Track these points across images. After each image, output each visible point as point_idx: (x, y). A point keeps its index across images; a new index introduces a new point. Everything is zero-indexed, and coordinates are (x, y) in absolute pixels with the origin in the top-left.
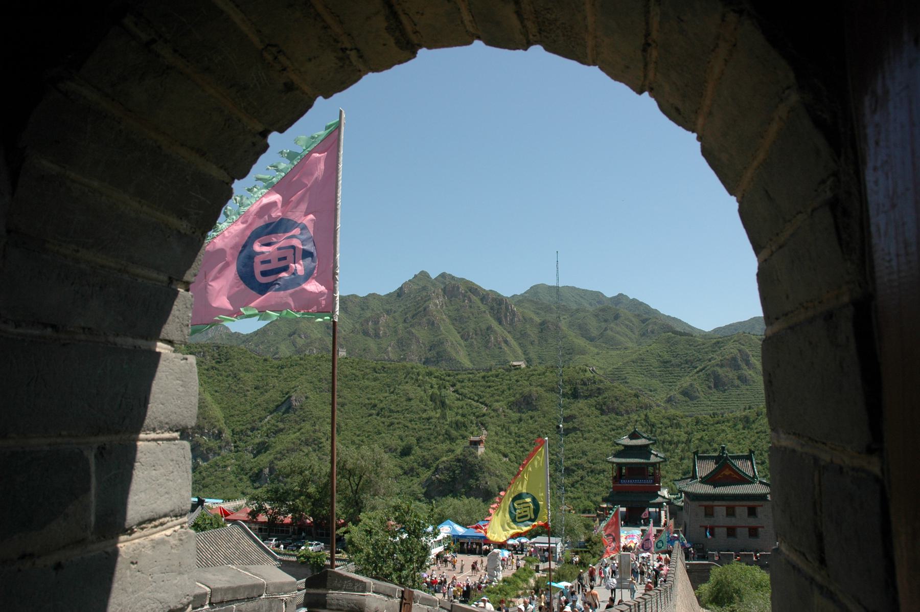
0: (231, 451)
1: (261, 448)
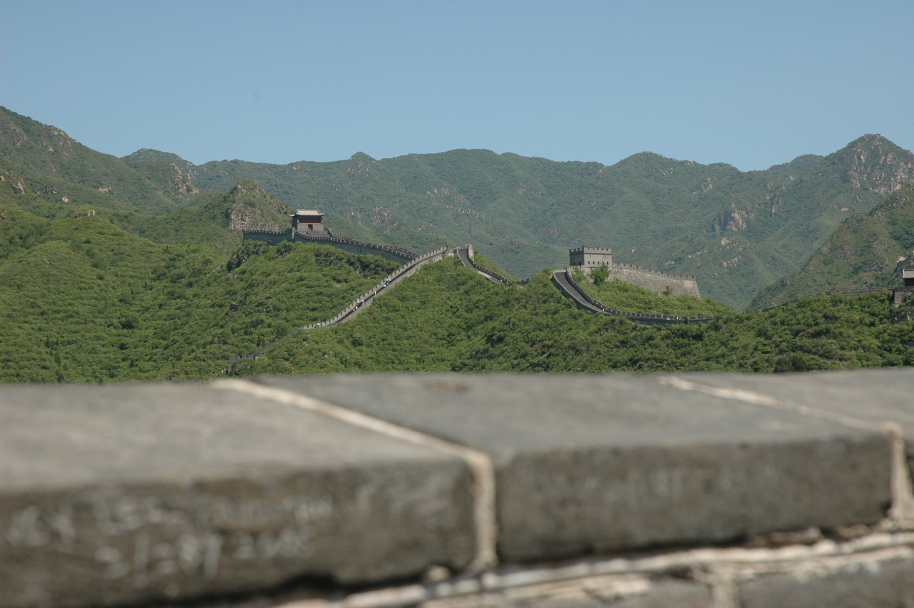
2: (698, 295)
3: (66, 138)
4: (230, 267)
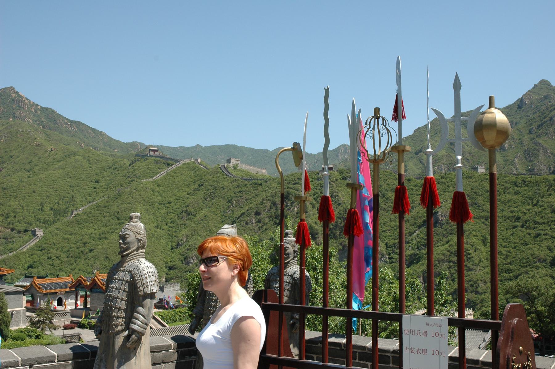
0: (386, 262)
2: (267, 174)
3: (106, 135)
4: (130, 165)
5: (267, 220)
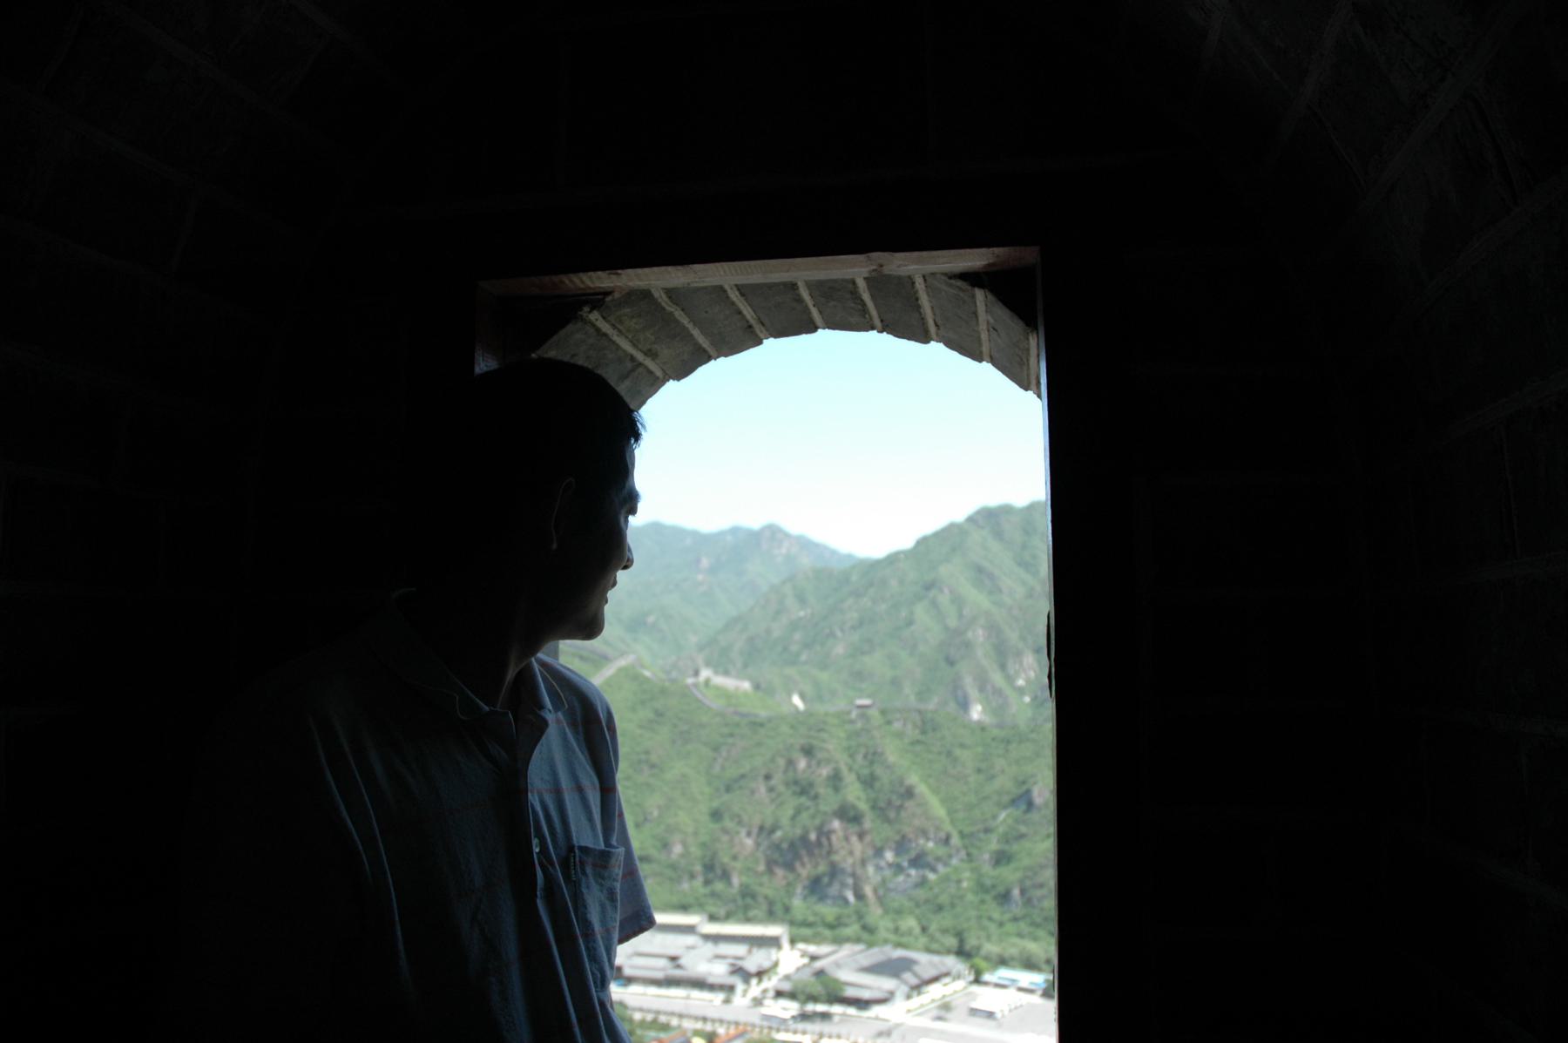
1: (1001, 858)
5: (781, 788)
